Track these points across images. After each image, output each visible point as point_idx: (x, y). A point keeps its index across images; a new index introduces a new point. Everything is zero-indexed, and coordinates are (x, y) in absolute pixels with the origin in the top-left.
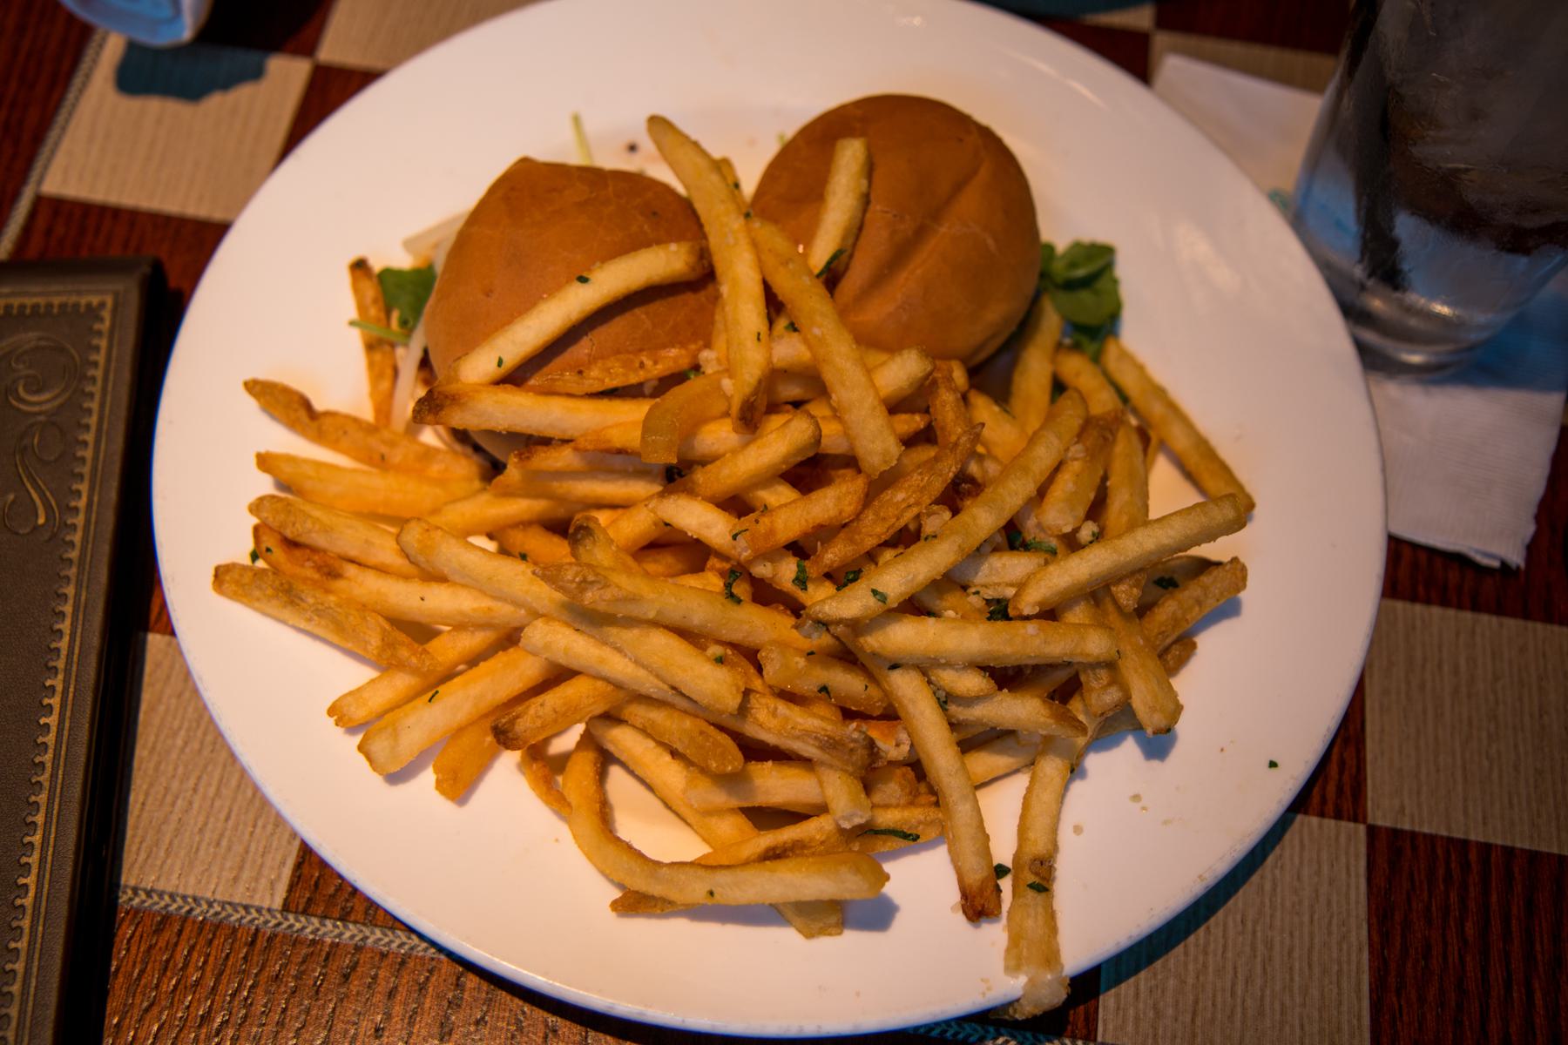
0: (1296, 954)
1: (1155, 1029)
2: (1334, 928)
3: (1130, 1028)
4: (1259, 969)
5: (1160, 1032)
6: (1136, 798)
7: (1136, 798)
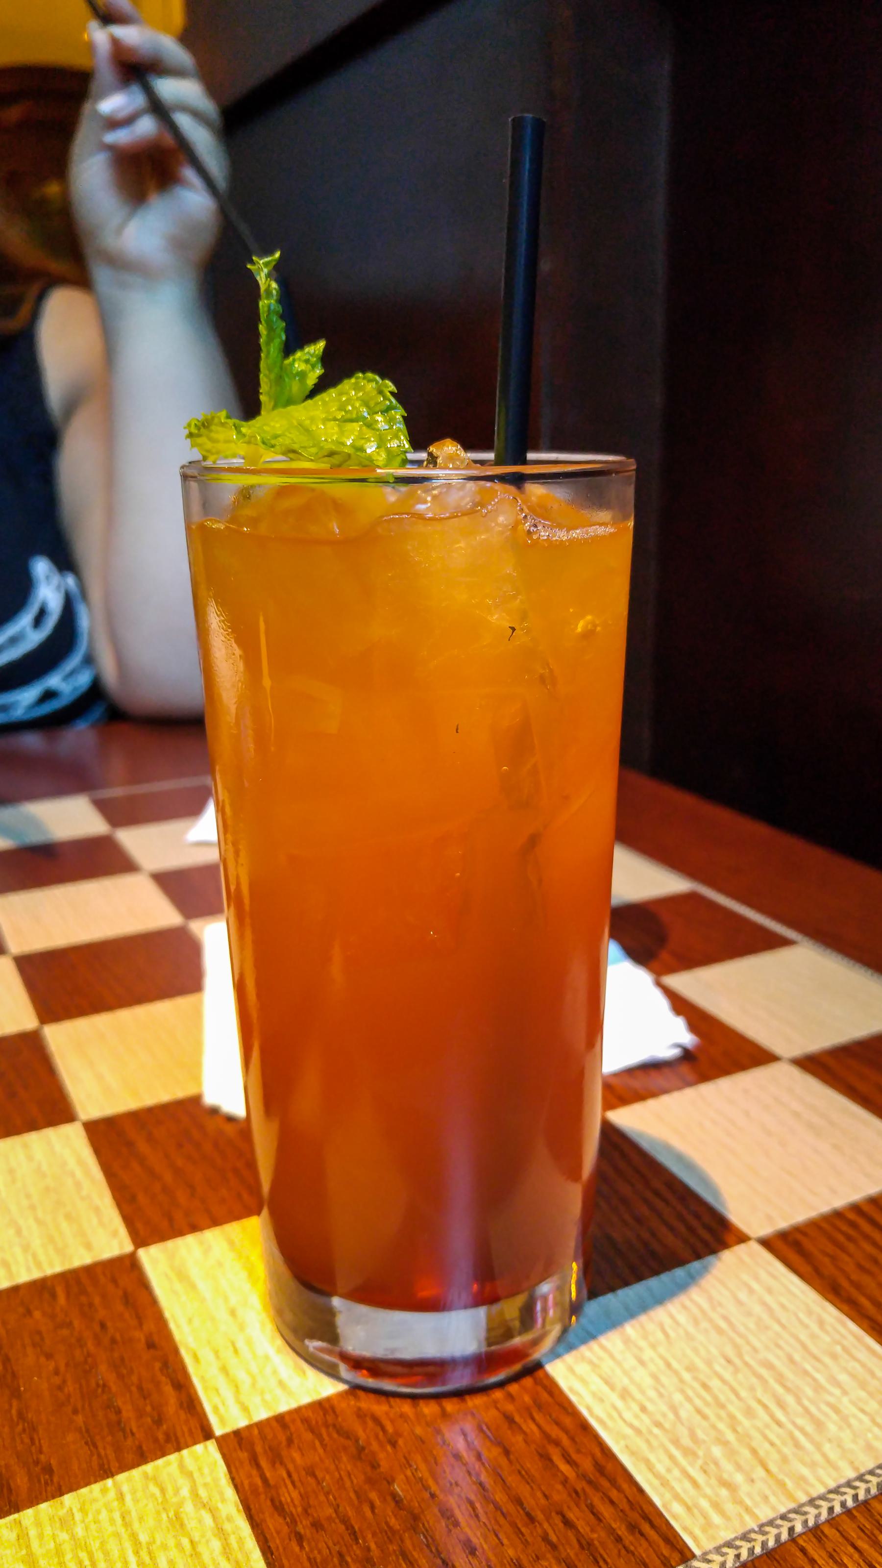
0: (797, 1357)
1: (741, 1503)
2: (806, 1320)
3: (716, 1519)
4: (780, 1390)
5: (749, 1502)
6: (514, 629)
7: (514, 629)
